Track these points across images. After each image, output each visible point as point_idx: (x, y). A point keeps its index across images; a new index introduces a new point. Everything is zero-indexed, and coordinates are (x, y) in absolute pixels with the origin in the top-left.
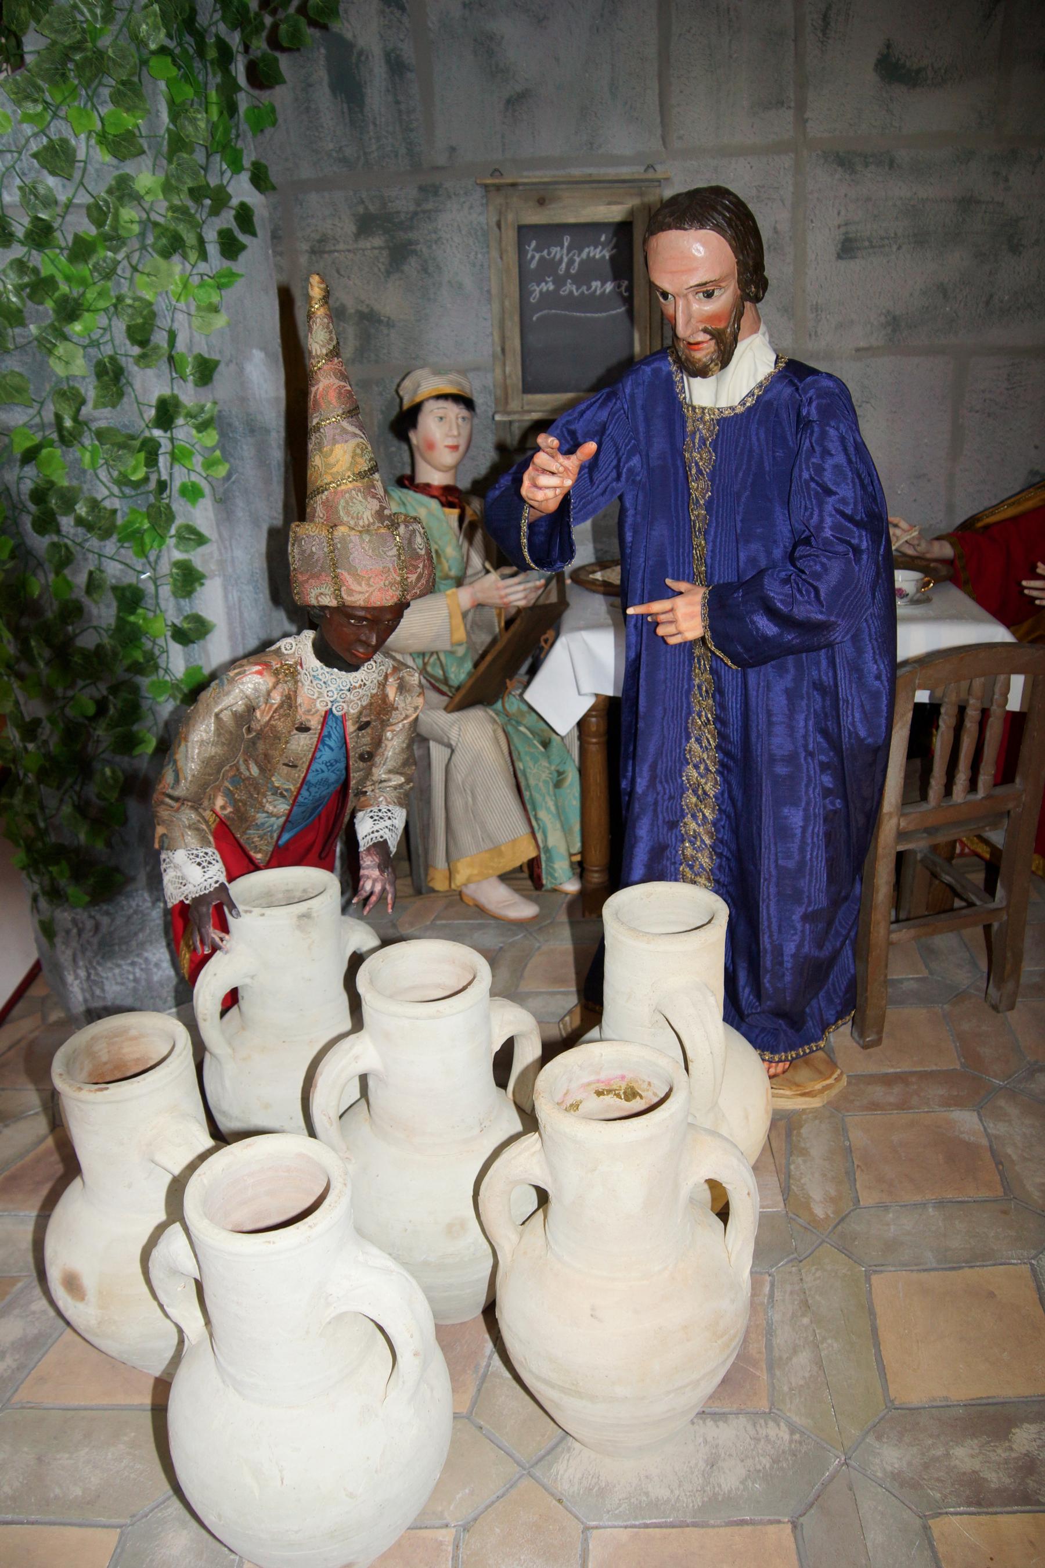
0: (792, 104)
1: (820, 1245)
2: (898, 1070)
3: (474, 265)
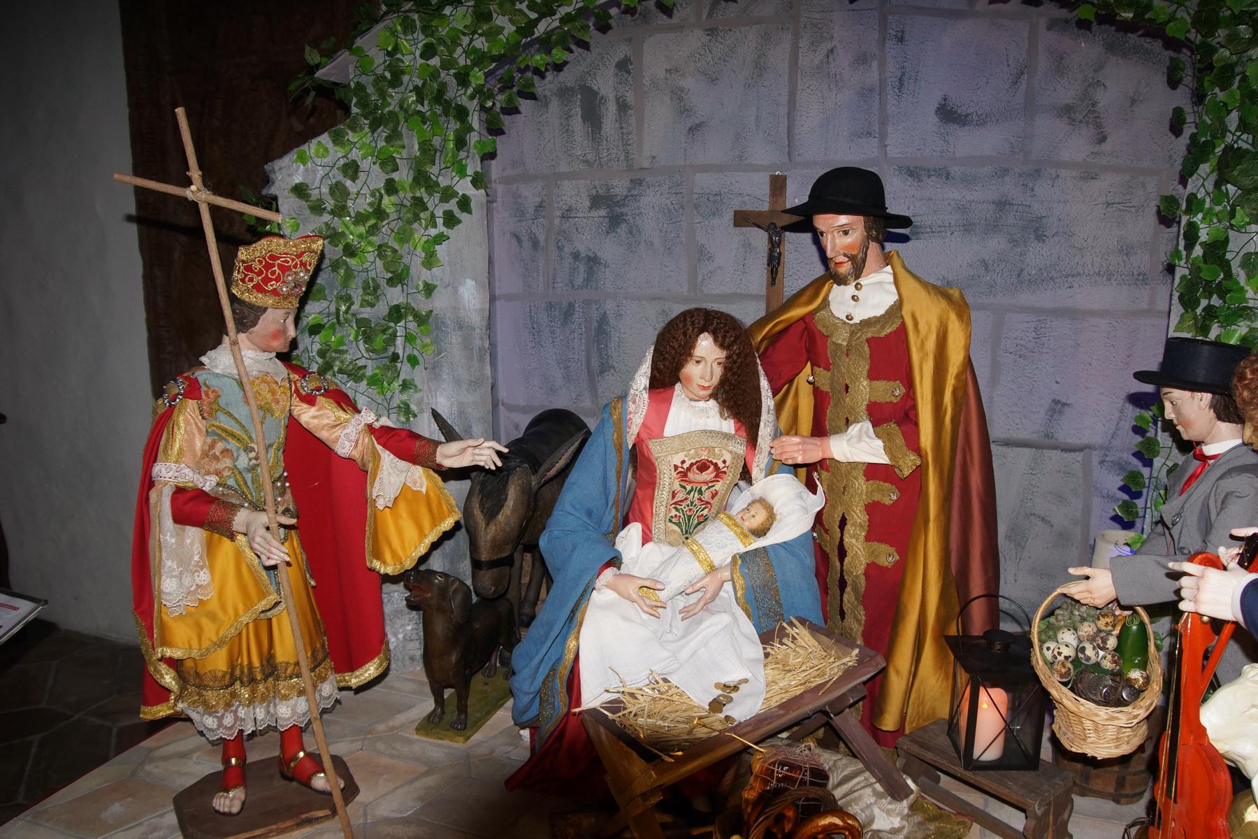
0: (877, 135)
3: (661, 231)
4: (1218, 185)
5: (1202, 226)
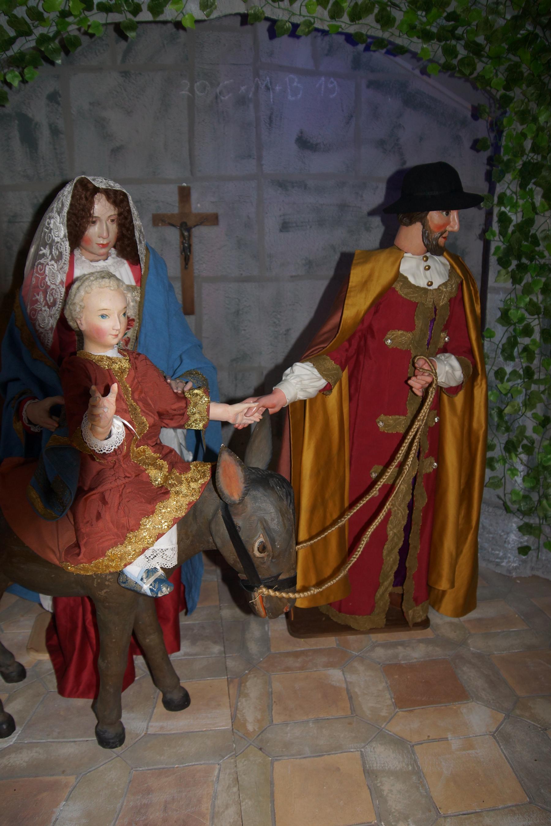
1: (248, 746)
2: (303, 649)
4: (523, 186)
5: (509, 214)
